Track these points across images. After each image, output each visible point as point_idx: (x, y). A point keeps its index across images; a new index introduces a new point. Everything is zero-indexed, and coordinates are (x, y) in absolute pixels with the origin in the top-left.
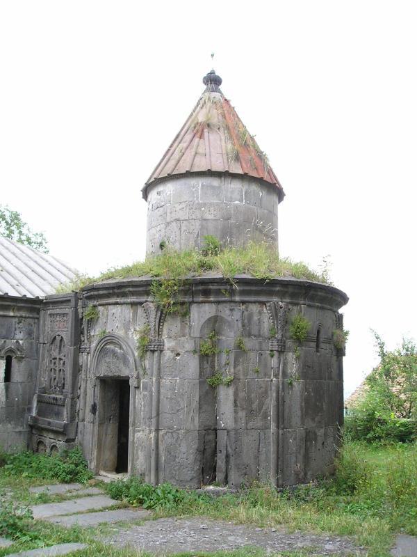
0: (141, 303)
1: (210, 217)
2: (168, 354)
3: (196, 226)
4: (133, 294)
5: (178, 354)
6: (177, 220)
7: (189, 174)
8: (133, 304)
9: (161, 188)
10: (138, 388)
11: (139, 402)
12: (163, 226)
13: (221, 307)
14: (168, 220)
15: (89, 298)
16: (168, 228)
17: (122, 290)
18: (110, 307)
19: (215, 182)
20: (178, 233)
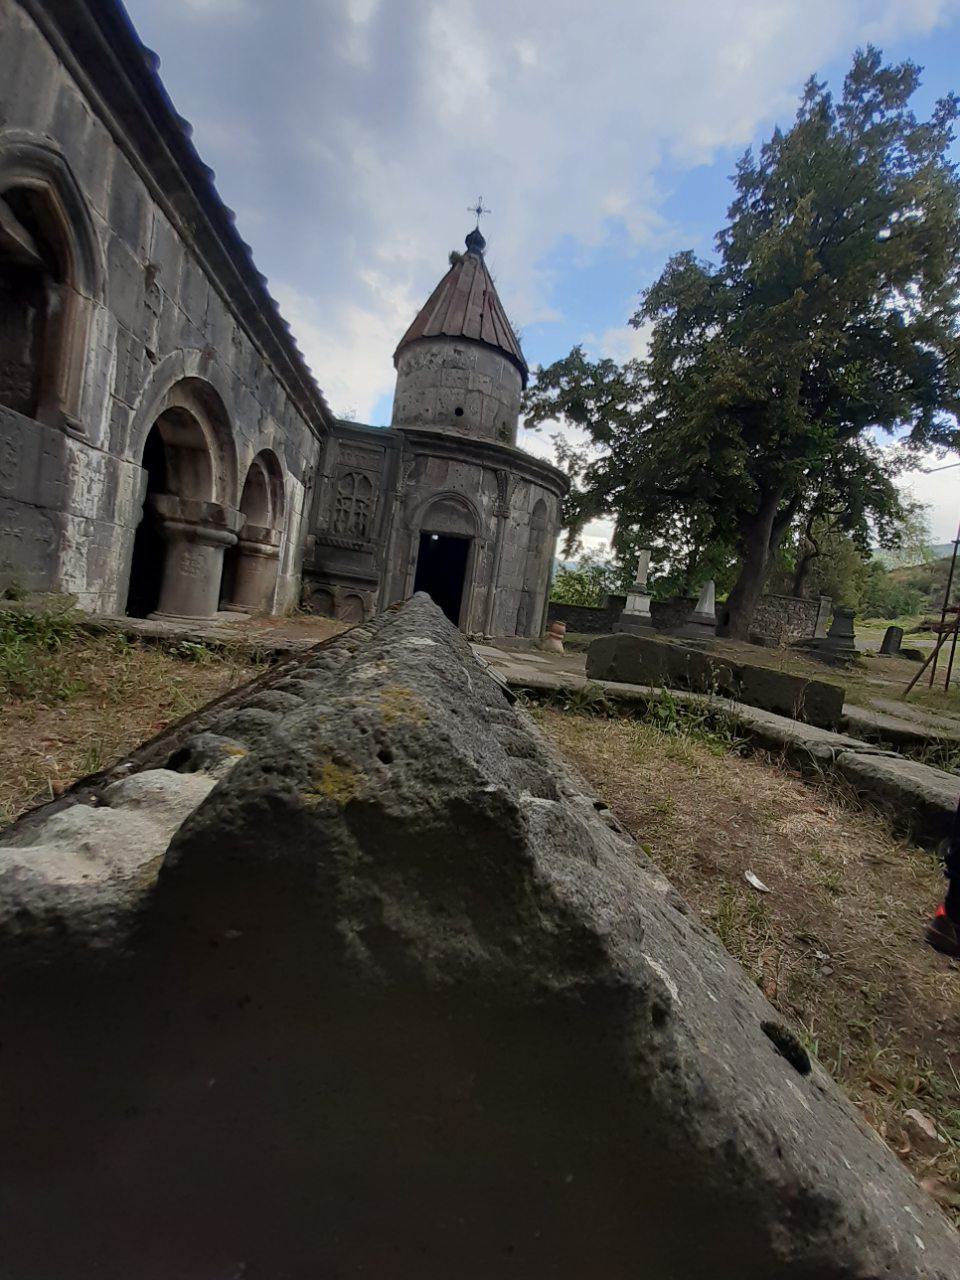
0: (495, 471)
1: (505, 402)
2: (511, 523)
3: (495, 406)
4: (490, 458)
5: (518, 525)
6: (480, 392)
7: (498, 349)
8: (485, 468)
9: (461, 347)
10: (483, 547)
11: (479, 559)
12: (462, 391)
13: (546, 492)
14: (470, 387)
15: (413, 443)
16: (469, 395)
17: (480, 451)
18: (450, 463)
19: (512, 369)
20: (480, 403)
